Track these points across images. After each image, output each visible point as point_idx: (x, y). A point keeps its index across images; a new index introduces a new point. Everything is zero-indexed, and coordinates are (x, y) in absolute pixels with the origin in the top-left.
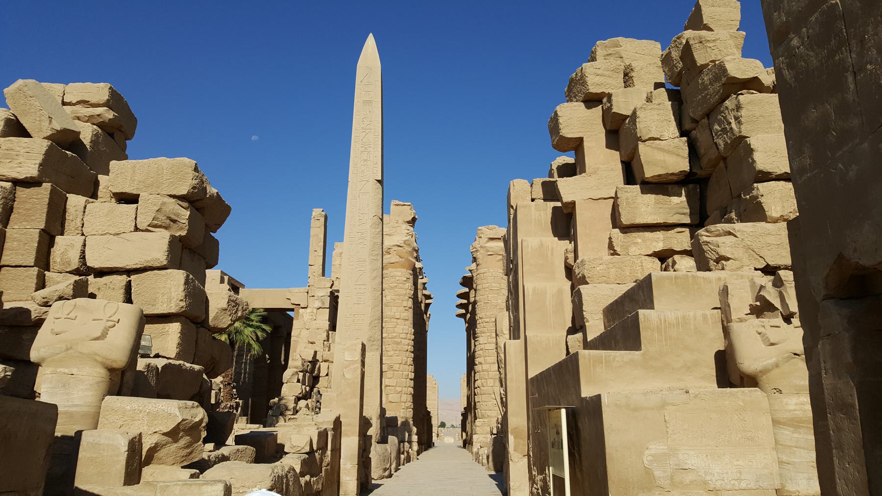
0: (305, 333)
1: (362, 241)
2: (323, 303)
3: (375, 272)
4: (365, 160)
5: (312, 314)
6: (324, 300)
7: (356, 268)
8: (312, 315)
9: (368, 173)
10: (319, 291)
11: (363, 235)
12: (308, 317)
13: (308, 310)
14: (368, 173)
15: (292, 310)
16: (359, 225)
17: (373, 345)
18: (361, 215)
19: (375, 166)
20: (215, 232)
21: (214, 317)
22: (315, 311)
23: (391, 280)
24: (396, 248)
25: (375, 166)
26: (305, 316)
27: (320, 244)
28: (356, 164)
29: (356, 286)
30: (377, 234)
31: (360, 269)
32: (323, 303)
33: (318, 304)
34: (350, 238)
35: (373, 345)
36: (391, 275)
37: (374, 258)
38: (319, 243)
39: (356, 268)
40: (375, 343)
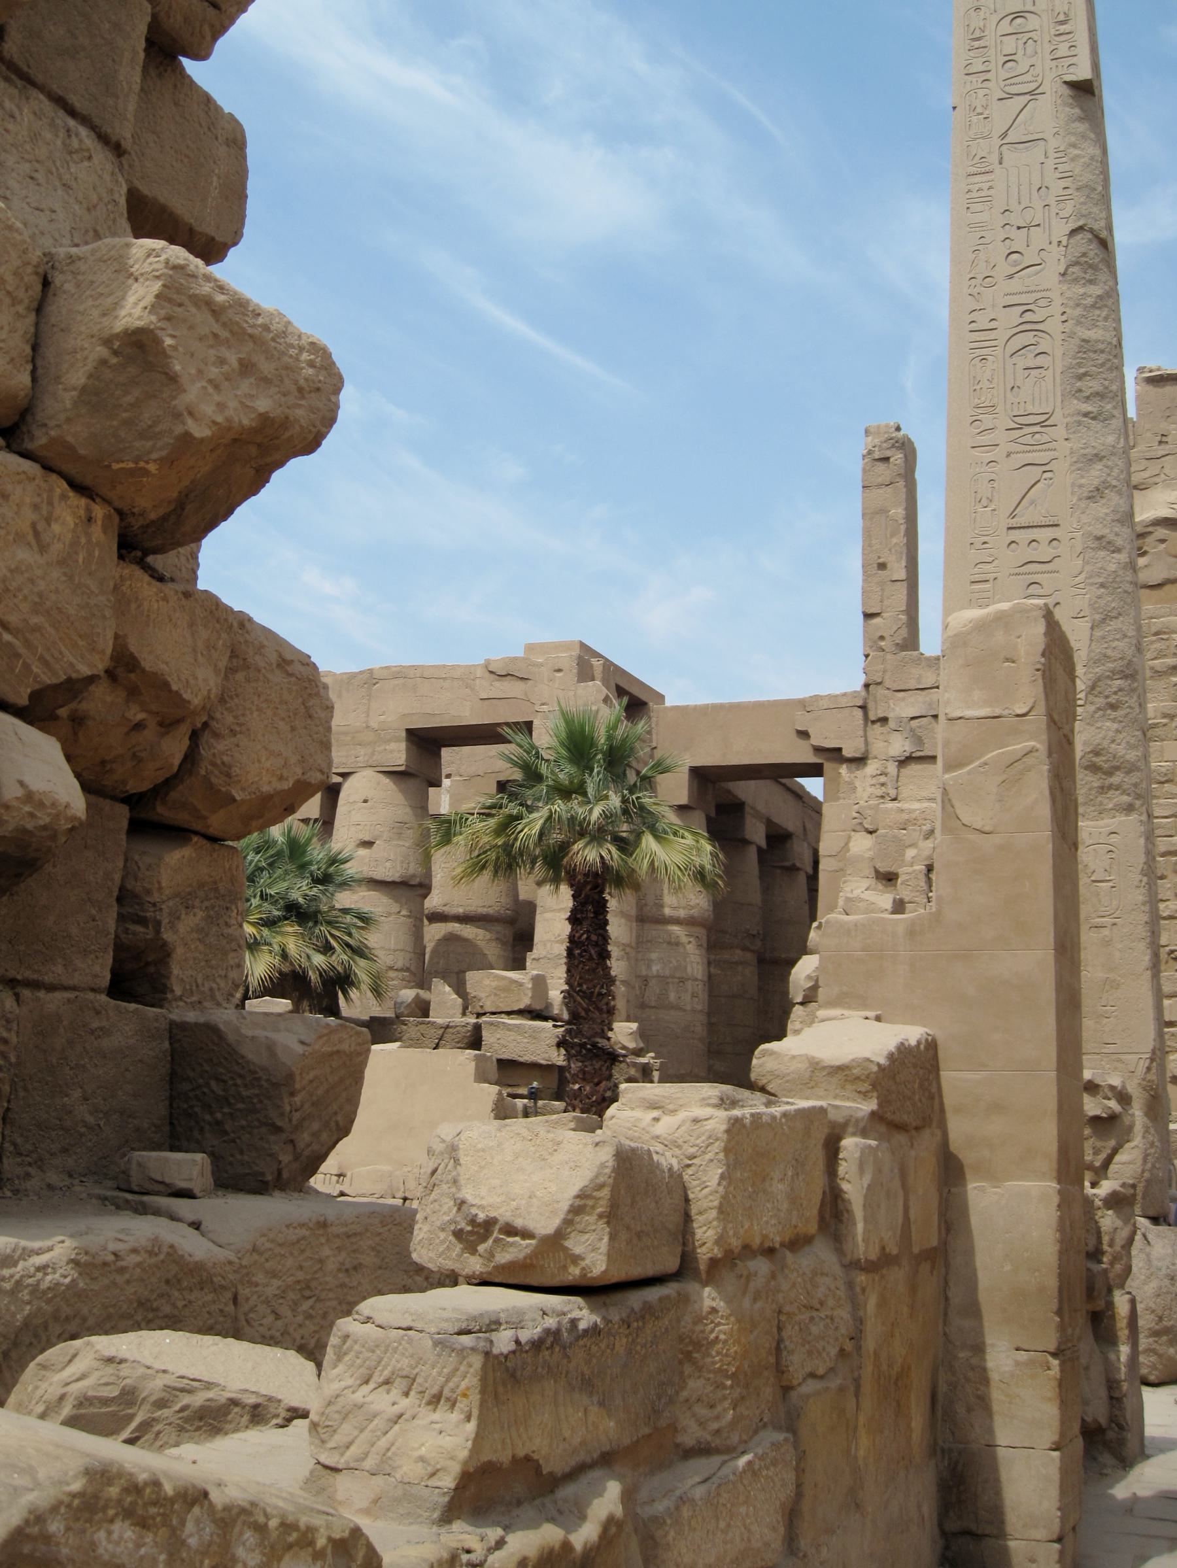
0: (861, 844)
1: (1028, 338)
2: (919, 741)
3: (1099, 466)
4: (1018, 15)
5: (883, 779)
6: (919, 732)
7: (1008, 455)
8: (883, 785)
9: (1032, 61)
10: (903, 699)
11: (1028, 317)
12: (871, 790)
13: (872, 767)
14: (1032, 61)
15: (815, 770)
16: (1011, 277)
17: (1110, 787)
18: (1013, 233)
19: (1063, 28)
20: (201, 55)
21: (84, 390)
22: (892, 768)
23: (1154, 646)
24: (1162, 532)
25: (1063, 28)
26: (859, 789)
27: (895, 540)
28: (977, 34)
29: (1015, 535)
30: (1093, 306)
31: (1030, 458)
32: (919, 741)
33: (899, 746)
34: (976, 337)
35: (1110, 787)
36: (1154, 630)
37: (1086, 407)
38: (892, 536)
39: (1008, 455)
40: (1115, 779)
